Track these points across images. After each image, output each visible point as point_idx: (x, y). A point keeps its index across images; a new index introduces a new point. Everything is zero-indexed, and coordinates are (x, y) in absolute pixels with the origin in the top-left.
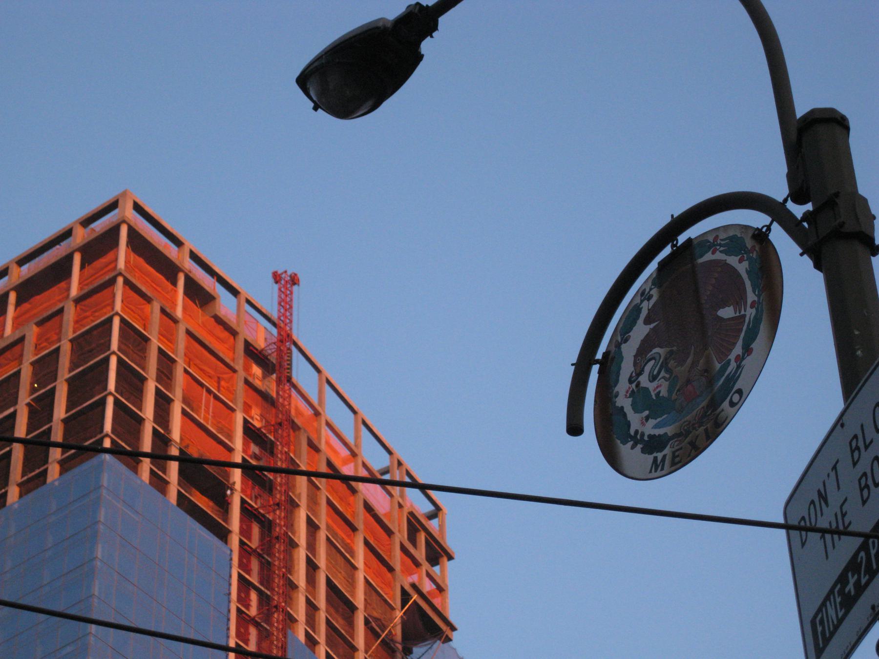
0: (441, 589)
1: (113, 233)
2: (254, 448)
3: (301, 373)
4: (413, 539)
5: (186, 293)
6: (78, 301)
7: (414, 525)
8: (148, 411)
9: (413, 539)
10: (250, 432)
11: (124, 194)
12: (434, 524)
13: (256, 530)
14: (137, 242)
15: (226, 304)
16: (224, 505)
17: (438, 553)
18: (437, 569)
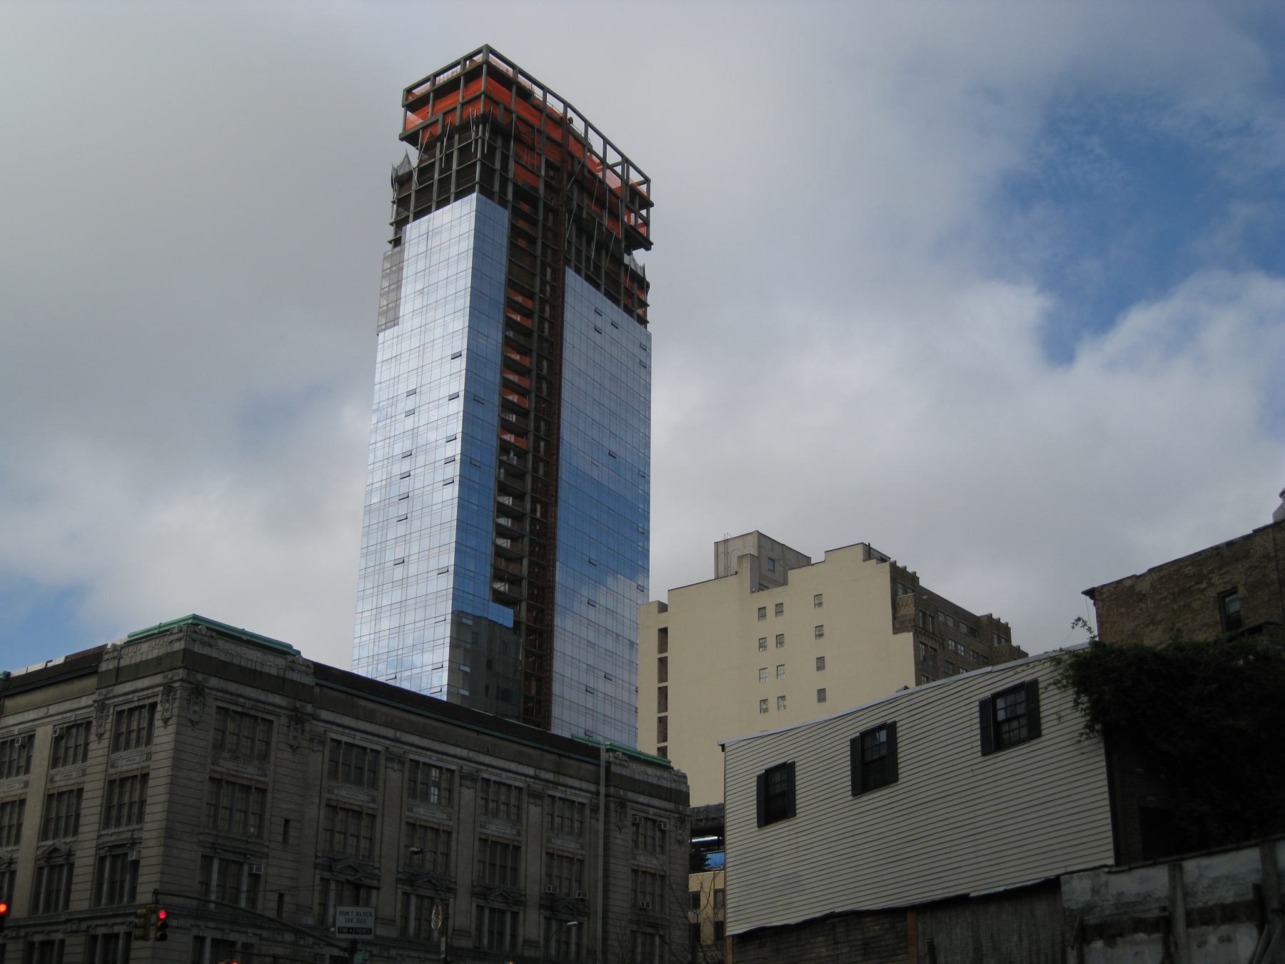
0: (646, 223)
1: (480, 67)
2: (551, 173)
3: (578, 126)
4: (632, 201)
5: (517, 94)
6: (463, 105)
7: (633, 191)
8: (498, 165)
9: (632, 201)
10: (549, 165)
11: (487, 46)
12: (643, 188)
13: (551, 217)
14: (494, 73)
15: (538, 93)
16: (535, 208)
17: (647, 204)
18: (644, 212)
